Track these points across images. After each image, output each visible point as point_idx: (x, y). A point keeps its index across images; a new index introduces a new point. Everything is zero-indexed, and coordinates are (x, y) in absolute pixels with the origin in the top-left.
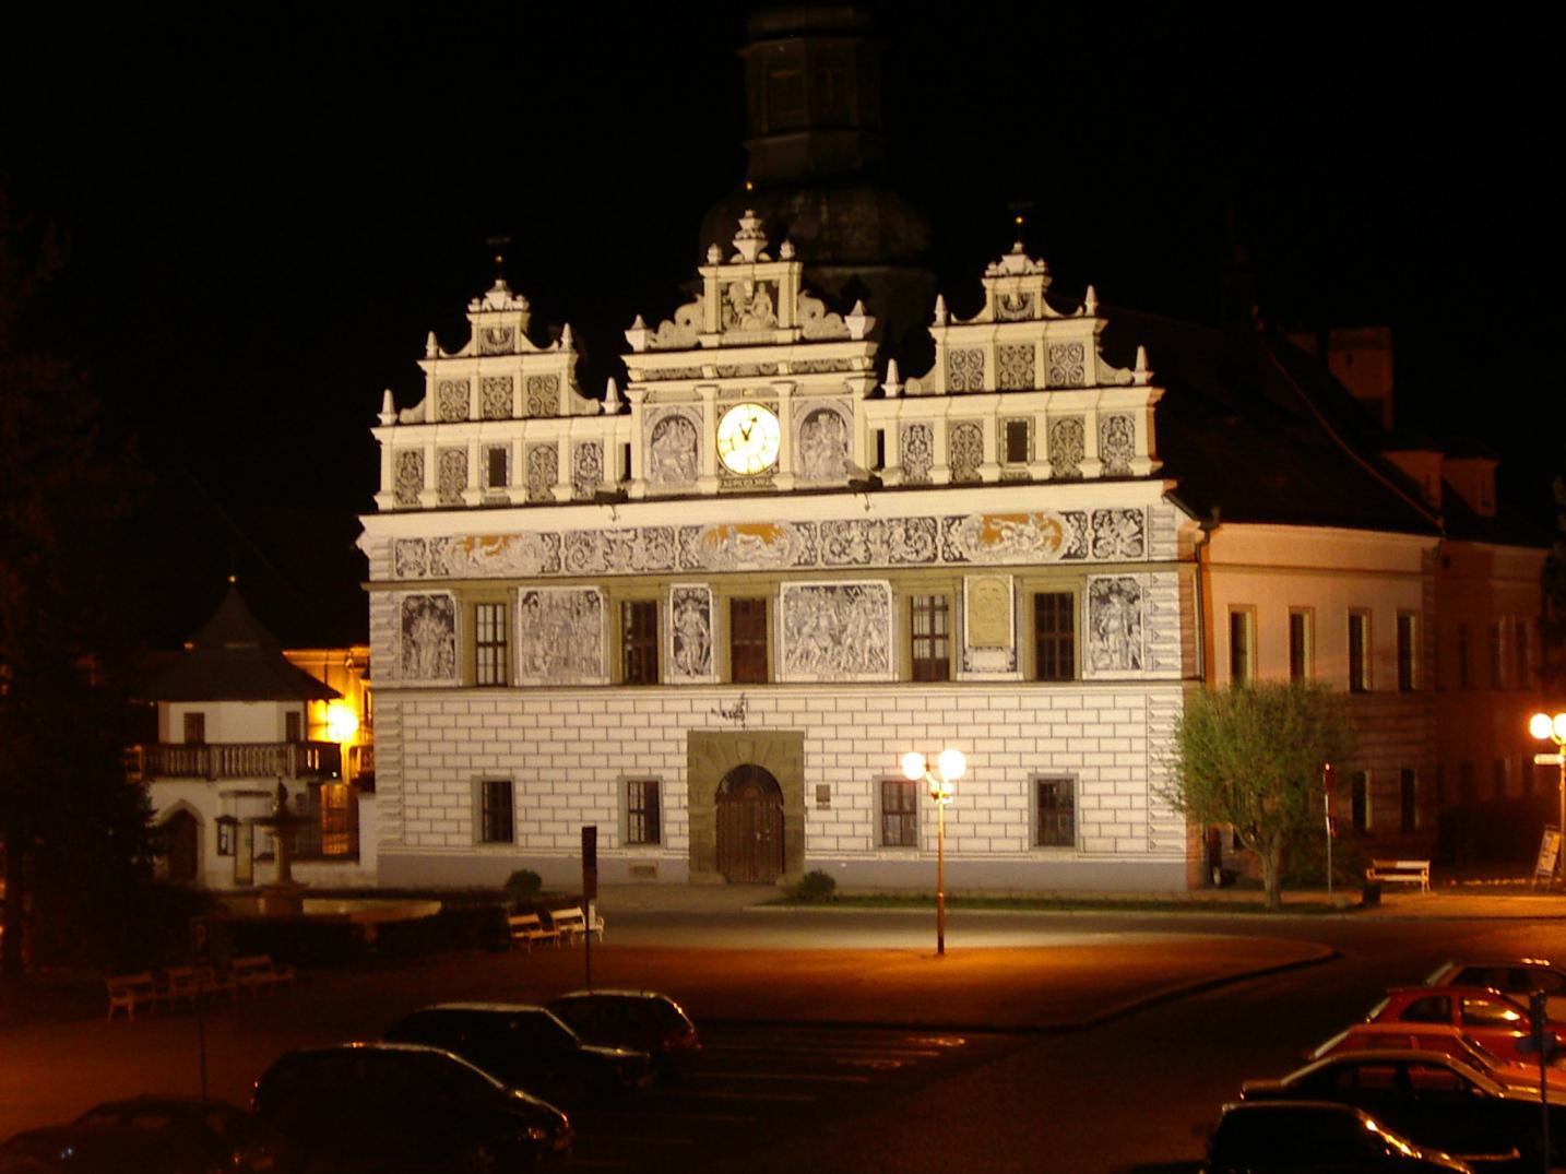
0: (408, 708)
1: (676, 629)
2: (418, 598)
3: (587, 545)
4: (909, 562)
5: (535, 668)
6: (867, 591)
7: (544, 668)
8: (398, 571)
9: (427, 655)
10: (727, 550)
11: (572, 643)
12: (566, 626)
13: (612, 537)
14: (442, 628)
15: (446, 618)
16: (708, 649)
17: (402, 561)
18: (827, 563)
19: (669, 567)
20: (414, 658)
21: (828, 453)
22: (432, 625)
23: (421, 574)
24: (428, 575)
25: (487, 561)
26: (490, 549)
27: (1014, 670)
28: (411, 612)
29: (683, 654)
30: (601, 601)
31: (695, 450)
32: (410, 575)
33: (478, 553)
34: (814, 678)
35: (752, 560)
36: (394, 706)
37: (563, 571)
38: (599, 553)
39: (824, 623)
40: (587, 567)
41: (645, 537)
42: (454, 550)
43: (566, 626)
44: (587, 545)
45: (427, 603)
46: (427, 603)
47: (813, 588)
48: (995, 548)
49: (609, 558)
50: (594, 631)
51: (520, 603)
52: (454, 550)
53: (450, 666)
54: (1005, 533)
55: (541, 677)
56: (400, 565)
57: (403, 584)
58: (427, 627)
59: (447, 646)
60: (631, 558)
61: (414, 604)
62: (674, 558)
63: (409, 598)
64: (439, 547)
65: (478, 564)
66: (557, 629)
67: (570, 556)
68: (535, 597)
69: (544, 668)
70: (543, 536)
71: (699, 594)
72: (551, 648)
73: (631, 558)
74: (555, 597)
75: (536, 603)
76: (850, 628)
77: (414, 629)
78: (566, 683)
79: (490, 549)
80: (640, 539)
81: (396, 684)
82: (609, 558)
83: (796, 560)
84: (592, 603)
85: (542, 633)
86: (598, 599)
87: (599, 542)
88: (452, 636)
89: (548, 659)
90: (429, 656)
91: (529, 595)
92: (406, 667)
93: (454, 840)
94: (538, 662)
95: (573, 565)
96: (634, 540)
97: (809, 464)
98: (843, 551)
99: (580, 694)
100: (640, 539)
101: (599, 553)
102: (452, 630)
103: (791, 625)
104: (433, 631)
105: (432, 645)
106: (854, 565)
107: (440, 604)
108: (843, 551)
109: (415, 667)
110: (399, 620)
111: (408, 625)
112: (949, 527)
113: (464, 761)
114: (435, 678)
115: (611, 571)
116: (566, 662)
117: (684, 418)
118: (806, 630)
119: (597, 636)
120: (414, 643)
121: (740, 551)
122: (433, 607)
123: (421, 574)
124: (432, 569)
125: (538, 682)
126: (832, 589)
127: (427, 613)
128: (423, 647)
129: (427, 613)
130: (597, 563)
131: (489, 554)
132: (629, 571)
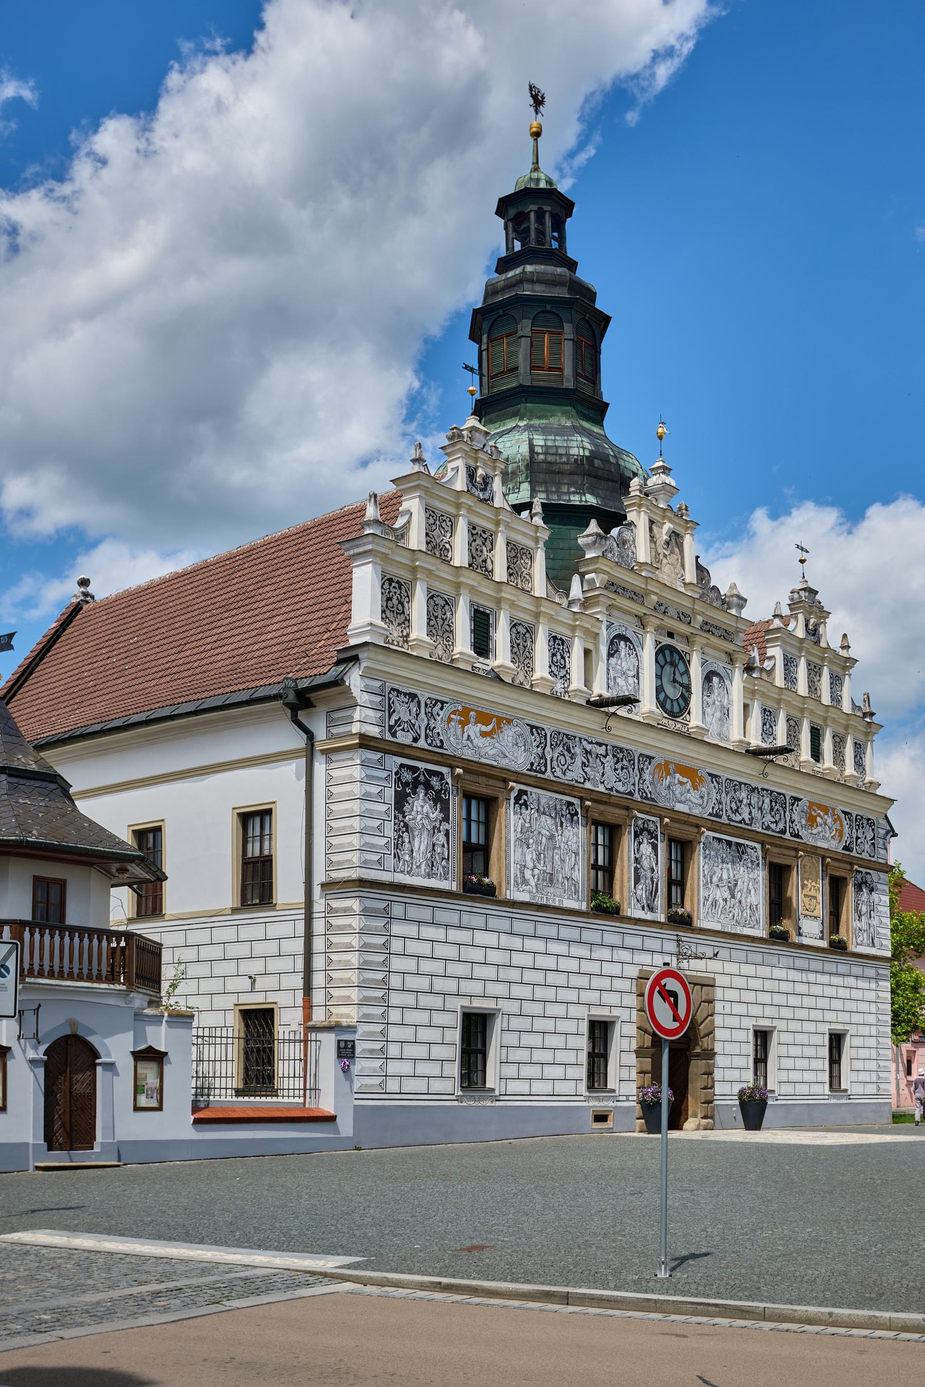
0: (397, 910)
1: (636, 859)
2: (414, 769)
3: (569, 750)
4: (773, 831)
5: (525, 881)
6: (749, 850)
7: (533, 882)
8: (391, 727)
9: (421, 844)
10: (669, 787)
11: (557, 857)
12: (552, 837)
13: (589, 747)
14: (436, 815)
15: (439, 800)
16: (657, 884)
17: (395, 717)
18: (729, 819)
19: (631, 794)
20: (407, 845)
21: (718, 714)
22: (427, 808)
23: (416, 740)
24: (422, 743)
25: (479, 742)
26: (484, 728)
27: (822, 938)
28: (406, 784)
29: (640, 887)
30: (579, 816)
31: (638, 678)
32: (404, 738)
33: (474, 730)
34: (718, 927)
35: (684, 802)
36: (382, 905)
37: (549, 775)
38: (579, 760)
39: (725, 876)
40: (570, 775)
41: (614, 756)
42: (450, 720)
43: (552, 837)
44: (569, 750)
45: (422, 778)
46: (422, 778)
47: (720, 840)
48: (814, 831)
49: (586, 769)
50: (574, 847)
51: (512, 801)
52: (450, 720)
53: (444, 863)
54: (819, 819)
55: (530, 892)
56: (392, 722)
57: (400, 750)
58: (420, 807)
59: (441, 838)
60: (603, 775)
61: (407, 776)
62: (634, 785)
63: (402, 766)
64: (435, 712)
65: (472, 742)
66: (544, 839)
67: (555, 759)
68: (525, 797)
69: (533, 882)
70: (532, 727)
71: (652, 827)
72: (539, 860)
73: (603, 775)
74: (543, 801)
75: (525, 804)
76: (739, 883)
77: (407, 808)
78: (551, 903)
79: (484, 728)
80: (610, 757)
81: (386, 877)
82: (586, 769)
83: (711, 811)
84: (572, 816)
85: (531, 841)
86: (576, 813)
87: (578, 750)
88: (444, 826)
89: (536, 871)
90: (423, 848)
91: (522, 793)
92: (397, 856)
93: (437, 1086)
94: (528, 874)
95: (558, 769)
96: (605, 757)
97: (708, 719)
98: (737, 811)
99: (541, 916)
100: (610, 757)
101: (579, 760)
102: (446, 819)
103: (706, 872)
104: (428, 816)
105: (426, 832)
106: (743, 826)
107: (435, 782)
108: (737, 811)
109: (407, 858)
110: (390, 794)
111: (401, 801)
112: (793, 805)
113: (450, 985)
114: (429, 876)
115: (588, 785)
116: (551, 881)
117: (631, 643)
118: (715, 879)
119: (576, 854)
120: (406, 825)
121: (678, 789)
122: (428, 787)
123: (416, 740)
124: (427, 736)
125: (524, 897)
126: (729, 843)
127: (421, 791)
128: (416, 833)
129: (421, 791)
130: (575, 773)
131: (484, 734)
132: (601, 788)
